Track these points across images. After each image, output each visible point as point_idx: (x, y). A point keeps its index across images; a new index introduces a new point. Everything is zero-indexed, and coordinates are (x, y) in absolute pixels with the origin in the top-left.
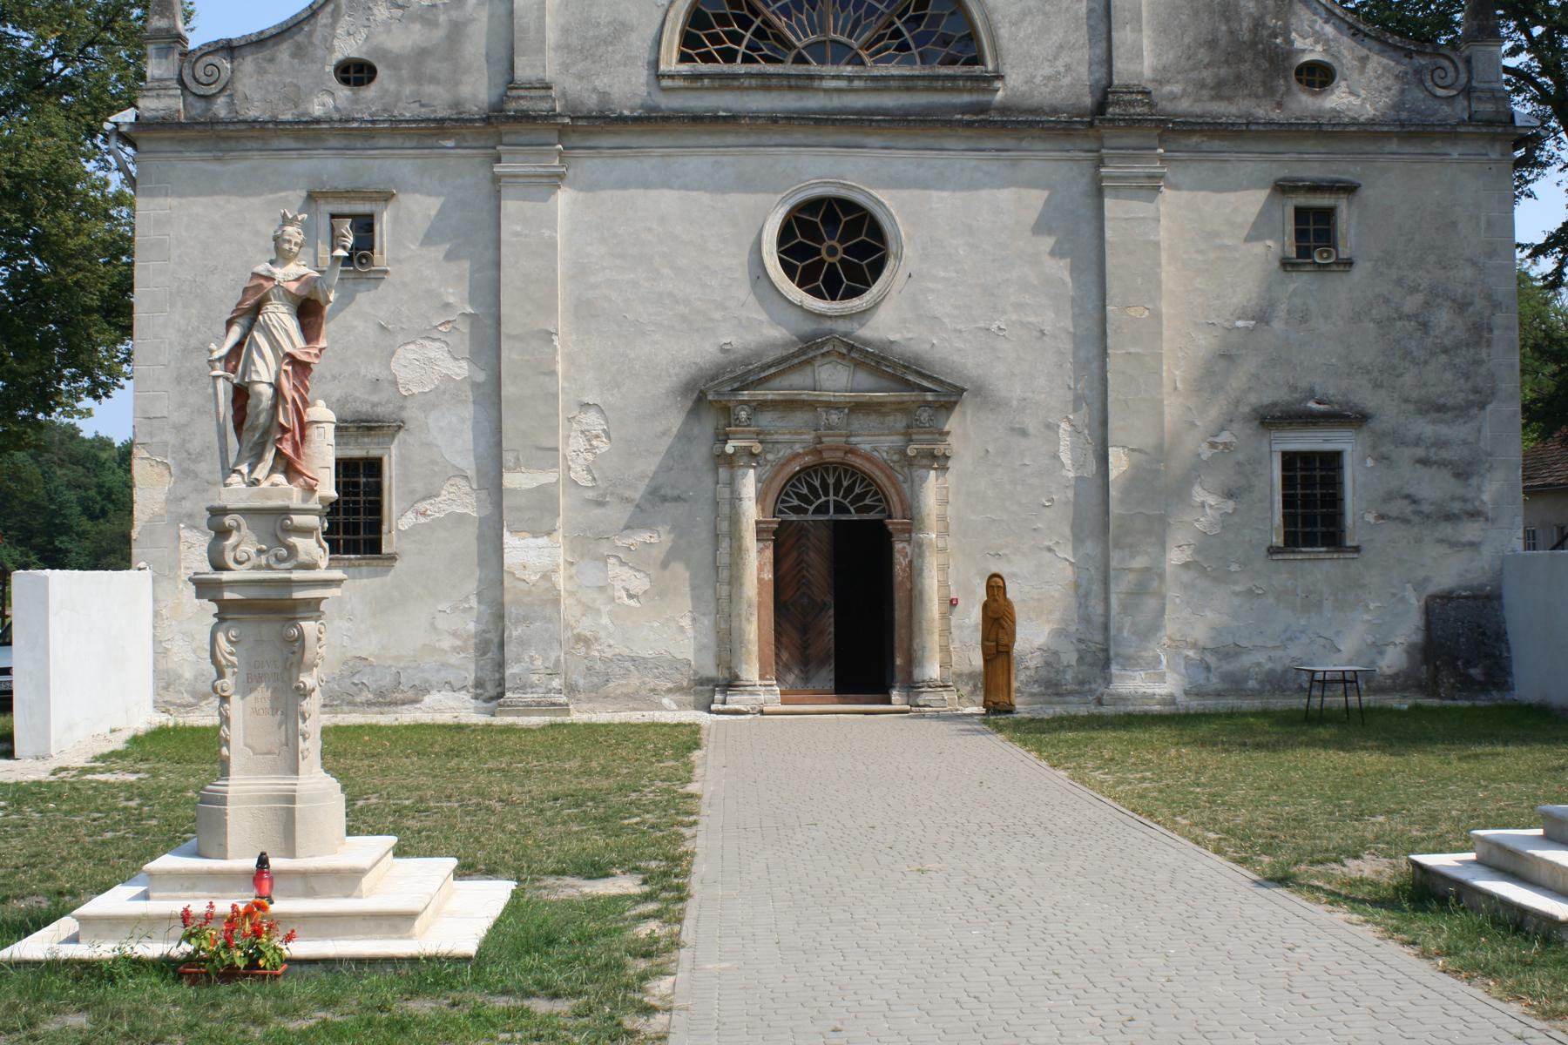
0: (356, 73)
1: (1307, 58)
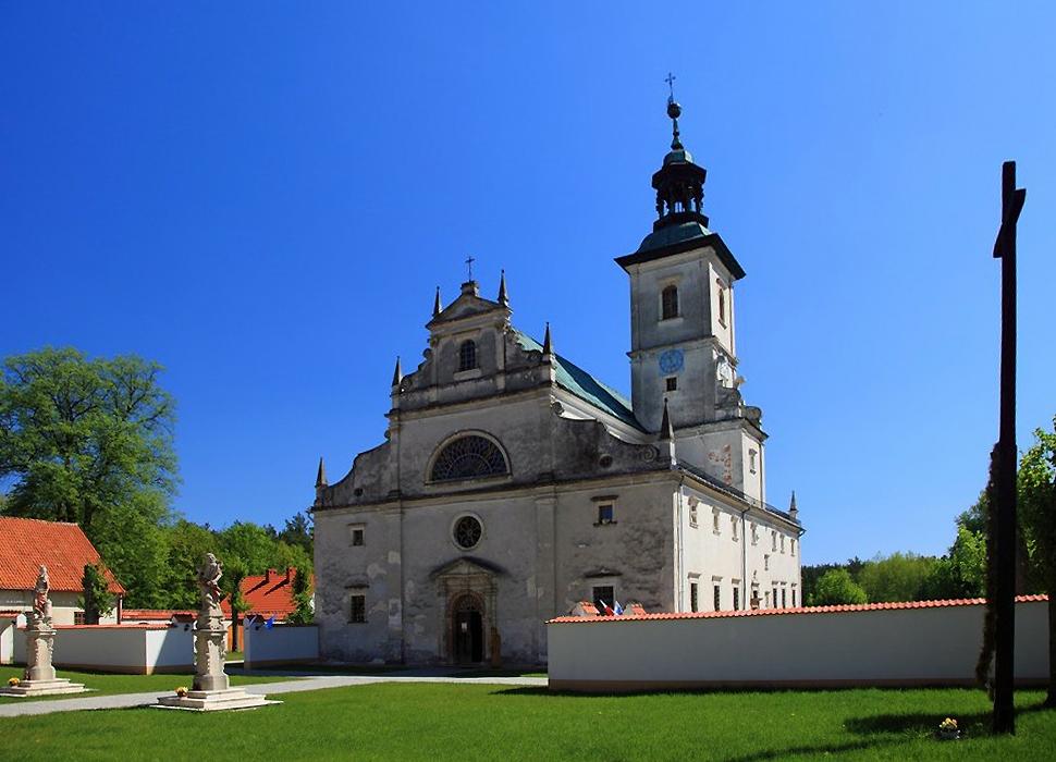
0: (358, 492)
1: (604, 455)
